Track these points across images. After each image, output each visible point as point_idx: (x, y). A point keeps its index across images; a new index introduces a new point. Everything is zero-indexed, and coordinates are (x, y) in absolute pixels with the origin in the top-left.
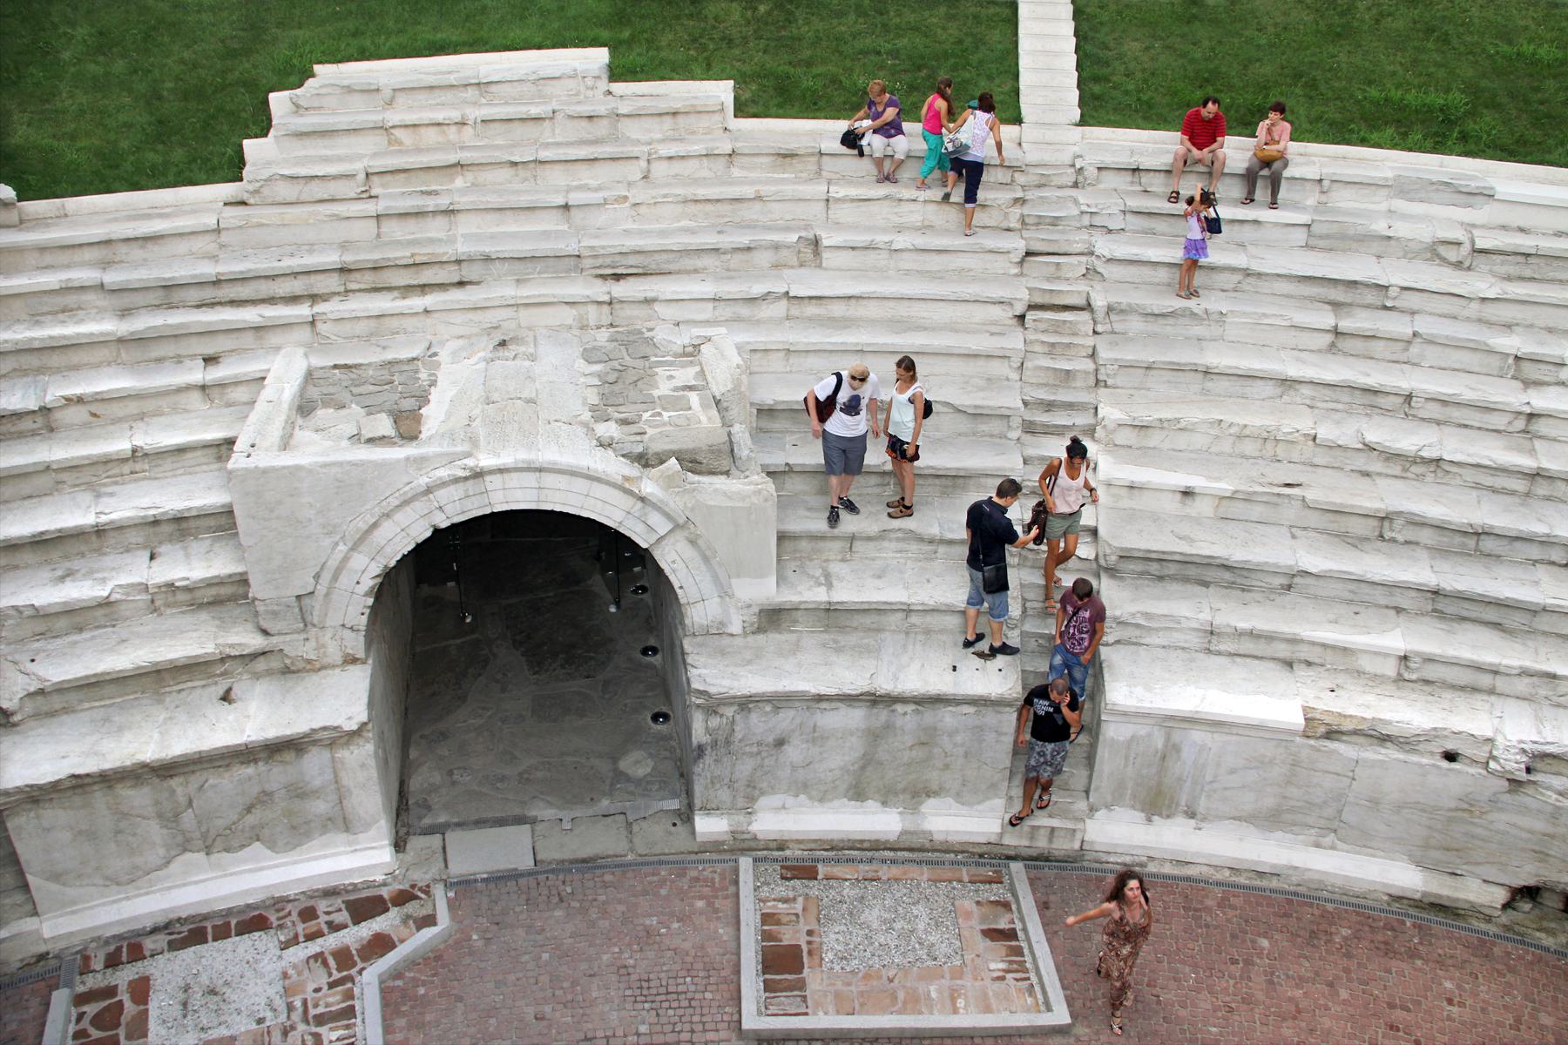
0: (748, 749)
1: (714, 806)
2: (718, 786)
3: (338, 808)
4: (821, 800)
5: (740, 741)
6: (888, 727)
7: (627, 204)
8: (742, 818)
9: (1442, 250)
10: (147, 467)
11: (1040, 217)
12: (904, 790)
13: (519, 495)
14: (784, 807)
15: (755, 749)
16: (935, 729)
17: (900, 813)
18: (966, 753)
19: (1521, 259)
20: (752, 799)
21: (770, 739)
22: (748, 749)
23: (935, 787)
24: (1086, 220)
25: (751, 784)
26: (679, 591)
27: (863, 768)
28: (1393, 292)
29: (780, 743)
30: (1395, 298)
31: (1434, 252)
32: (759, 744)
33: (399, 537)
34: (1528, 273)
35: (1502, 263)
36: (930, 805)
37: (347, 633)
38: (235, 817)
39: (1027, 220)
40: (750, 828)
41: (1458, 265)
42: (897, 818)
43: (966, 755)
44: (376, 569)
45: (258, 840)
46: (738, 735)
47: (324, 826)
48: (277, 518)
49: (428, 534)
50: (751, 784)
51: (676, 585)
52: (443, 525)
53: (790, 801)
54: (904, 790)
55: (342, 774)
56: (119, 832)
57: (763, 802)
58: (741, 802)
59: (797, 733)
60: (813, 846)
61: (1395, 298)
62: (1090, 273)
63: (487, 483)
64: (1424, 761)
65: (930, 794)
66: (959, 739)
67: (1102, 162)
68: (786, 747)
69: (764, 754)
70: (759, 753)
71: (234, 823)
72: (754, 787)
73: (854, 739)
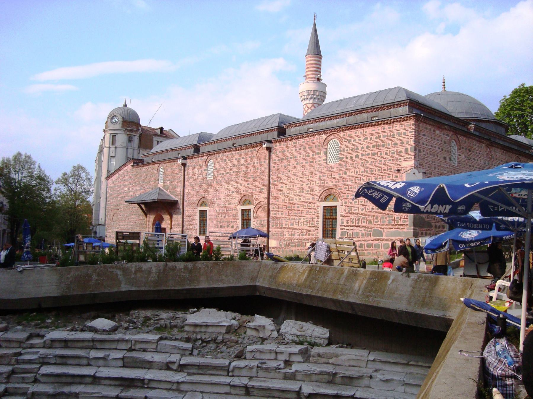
9: (171, 366)
11: (24, 360)
19: (197, 367)
24: (41, 360)
28: (146, 382)
30: (148, 384)
31: (167, 367)
34: (200, 372)
35: (191, 369)
39: (19, 361)
41: (176, 371)
61: (148, 384)
62: (36, 381)
67: (52, 338)
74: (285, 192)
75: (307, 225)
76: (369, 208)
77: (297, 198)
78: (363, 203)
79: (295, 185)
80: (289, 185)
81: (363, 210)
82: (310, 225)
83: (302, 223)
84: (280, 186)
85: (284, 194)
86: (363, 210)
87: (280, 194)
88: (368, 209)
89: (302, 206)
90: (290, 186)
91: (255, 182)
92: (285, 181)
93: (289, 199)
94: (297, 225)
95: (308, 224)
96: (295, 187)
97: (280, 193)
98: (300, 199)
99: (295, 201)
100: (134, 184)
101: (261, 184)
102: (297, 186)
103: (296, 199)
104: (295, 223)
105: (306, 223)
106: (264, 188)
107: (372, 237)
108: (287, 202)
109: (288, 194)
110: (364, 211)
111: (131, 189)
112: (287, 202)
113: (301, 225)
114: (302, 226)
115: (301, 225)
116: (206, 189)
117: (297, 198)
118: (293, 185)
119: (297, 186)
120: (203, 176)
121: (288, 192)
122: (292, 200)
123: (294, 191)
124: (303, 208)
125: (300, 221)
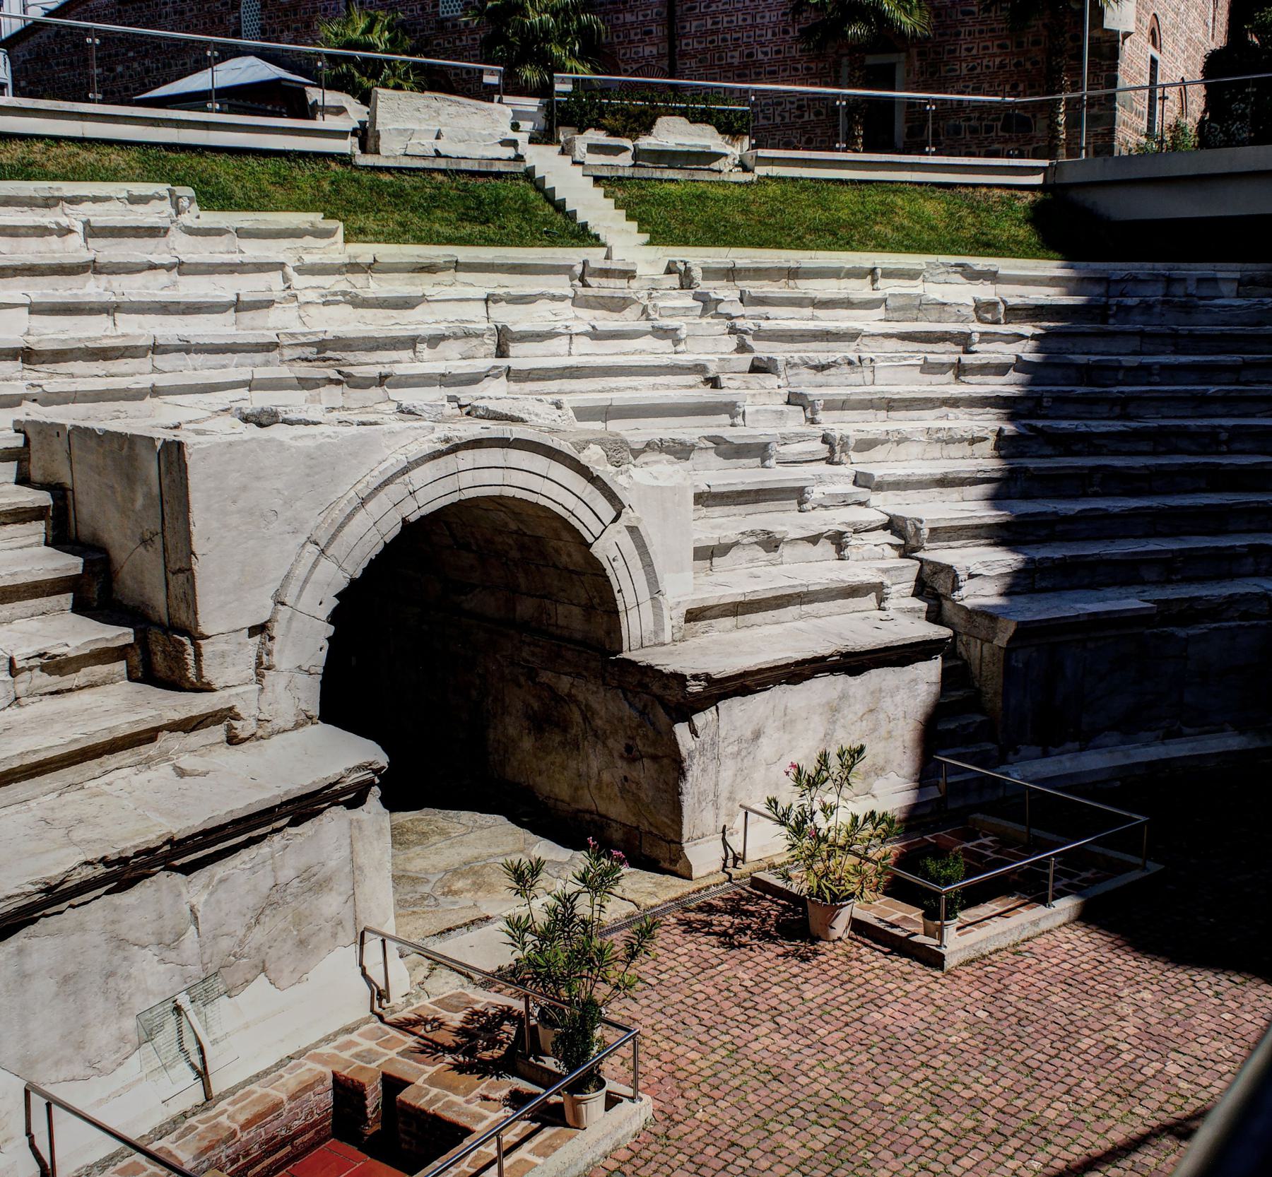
3: (350, 903)
21: (748, 734)
26: (618, 596)
29: (757, 735)
33: (370, 534)
37: (302, 679)
46: (722, 733)
47: (334, 935)
48: (239, 512)
51: (616, 589)
52: (413, 518)
55: (358, 846)
56: (111, 974)
59: (771, 721)
64: (1233, 624)
68: (761, 740)
69: (744, 753)
70: (739, 752)
72: (734, 800)
73: (816, 718)
74: (728, 36)
75: (802, 116)
76: (991, 64)
77: (768, 49)
78: (974, 52)
79: (758, 16)
80: (741, 17)
81: (974, 68)
82: (812, 117)
83: (787, 115)
84: (710, 22)
85: (724, 40)
86: (974, 68)
87: (712, 42)
88: (988, 67)
89: (785, 70)
90: (745, 20)
91: (621, 16)
92: (727, 7)
93: (741, 54)
94: (768, 119)
95: (806, 115)
96: (759, 20)
97: (709, 39)
98: (778, 52)
99: (761, 56)
100: (131, 54)
101: (641, 18)
102: (767, 20)
103: (766, 54)
104: (761, 115)
105: (797, 113)
106: (654, 29)
107: (1000, 134)
108: (736, 61)
109: (737, 39)
110: (978, 70)
111: (119, 69)
112: (736, 61)
113: (783, 118)
114: (787, 120)
115: (783, 118)
116: (438, 44)
117: (768, 49)
118: (754, 17)
119: (767, 20)
120: (423, 9)
121: (735, 35)
122: (750, 55)
123: (758, 32)
124: (787, 73)
125: (780, 108)
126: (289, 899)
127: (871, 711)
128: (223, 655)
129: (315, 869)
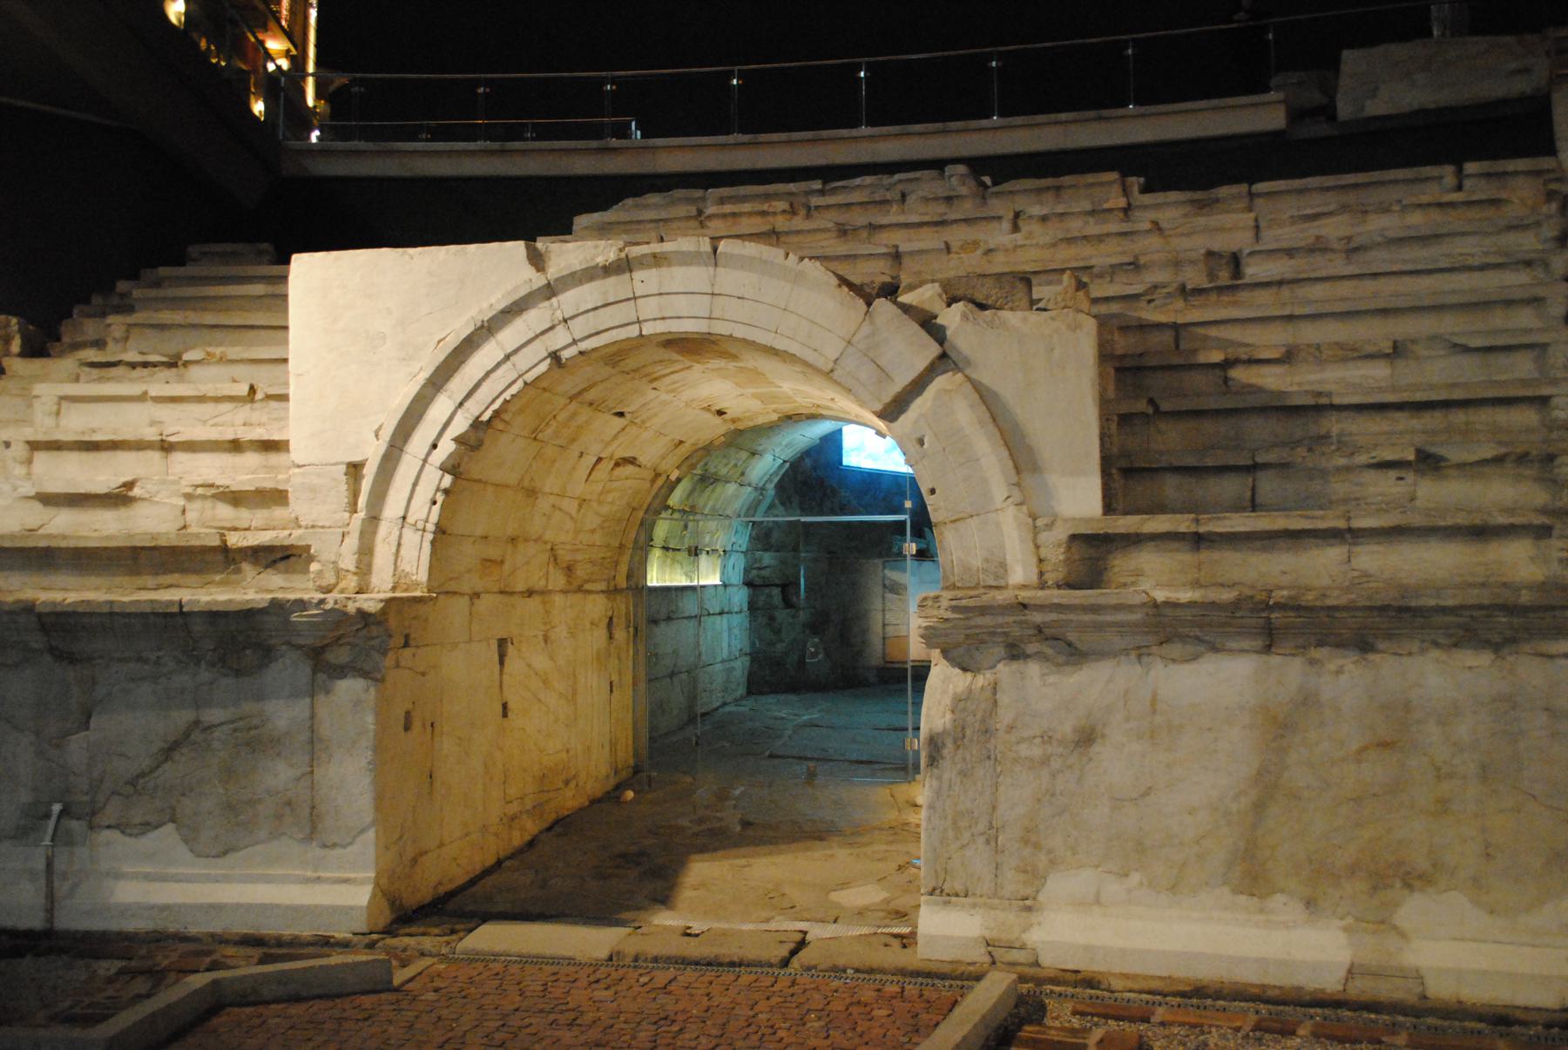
0: (1024, 750)
1: (958, 887)
2: (967, 835)
4: (1173, 889)
5: (1010, 728)
6: (1307, 701)
7: (979, 252)
8: (1011, 917)
10: (264, 419)
12: (1353, 870)
13: (681, 305)
14: (1097, 901)
15: (1037, 752)
16: (1407, 707)
17: (1346, 929)
18: (1484, 767)
20: (1034, 876)
21: (1067, 728)
22: (1024, 750)
23: (1423, 864)
25: (1029, 838)
27: (1259, 807)
29: (1087, 738)
32: (1046, 738)
36: (1413, 910)
38: (146, 763)
40: (1025, 937)
42: (1342, 938)
43: (1485, 773)
44: (461, 425)
45: (173, 820)
46: (1005, 716)
47: (279, 817)
49: (543, 367)
50: (1029, 838)
53: (1113, 888)
54: (1353, 870)
57: (1058, 886)
58: (1012, 882)
60: (1155, 985)
63: (637, 284)
65: (1413, 880)
66: (1463, 731)
68: (1096, 748)
69: (1056, 764)
70: (1045, 761)
71: (142, 775)
72: (1037, 846)
126: (216, 745)
127: (1384, 745)
128: (313, 490)
129: (255, 721)
